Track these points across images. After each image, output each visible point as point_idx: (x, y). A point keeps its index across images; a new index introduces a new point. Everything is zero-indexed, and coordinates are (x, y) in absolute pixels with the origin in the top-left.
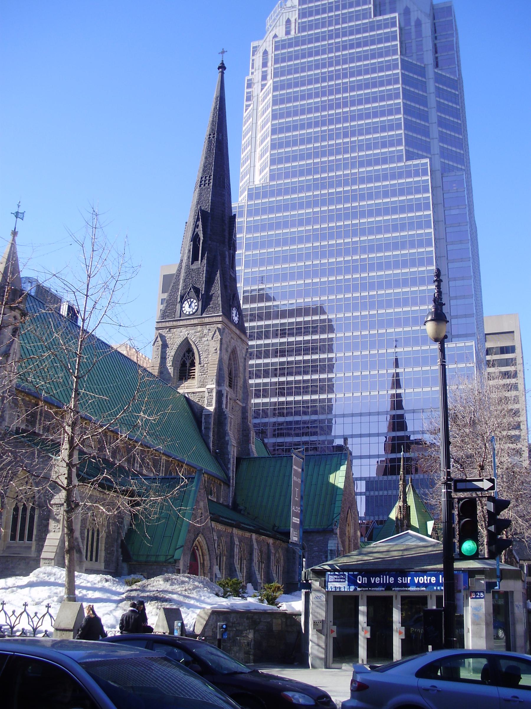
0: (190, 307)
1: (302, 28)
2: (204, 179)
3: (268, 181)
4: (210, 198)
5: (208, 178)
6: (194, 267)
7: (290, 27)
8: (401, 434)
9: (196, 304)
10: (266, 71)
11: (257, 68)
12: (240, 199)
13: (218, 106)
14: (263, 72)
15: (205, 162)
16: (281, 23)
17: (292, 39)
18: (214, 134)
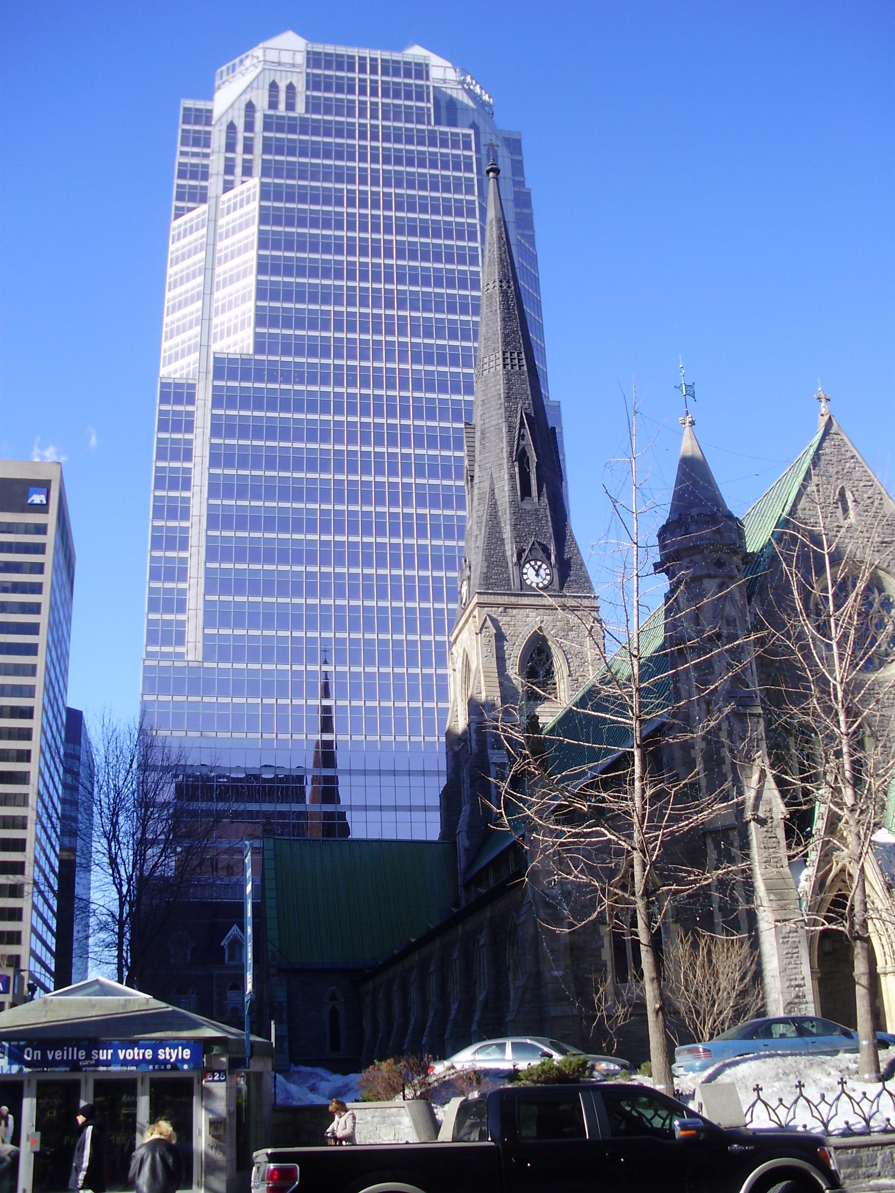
0: (537, 575)
1: (313, 105)
2: (508, 355)
3: (251, 352)
4: (529, 393)
5: (515, 355)
6: (527, 506)
7: (277, 96)
8: (329, 808)
9: (548, 571)
10: (233, 160)
11: (216, 149)
12: (164, 371)
13: (504, 236)
14: (227, 159)
15: (505, 328)
16: (261, 86)
17: (294, 119)
18: (508, 282)
